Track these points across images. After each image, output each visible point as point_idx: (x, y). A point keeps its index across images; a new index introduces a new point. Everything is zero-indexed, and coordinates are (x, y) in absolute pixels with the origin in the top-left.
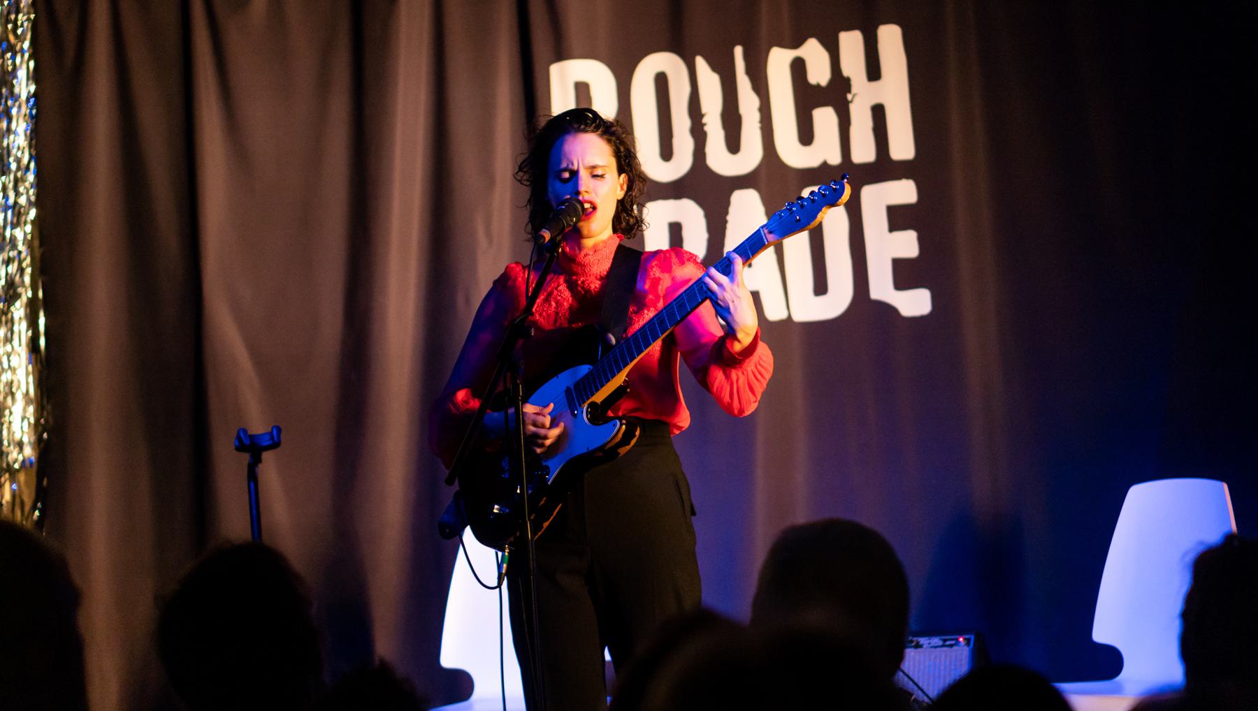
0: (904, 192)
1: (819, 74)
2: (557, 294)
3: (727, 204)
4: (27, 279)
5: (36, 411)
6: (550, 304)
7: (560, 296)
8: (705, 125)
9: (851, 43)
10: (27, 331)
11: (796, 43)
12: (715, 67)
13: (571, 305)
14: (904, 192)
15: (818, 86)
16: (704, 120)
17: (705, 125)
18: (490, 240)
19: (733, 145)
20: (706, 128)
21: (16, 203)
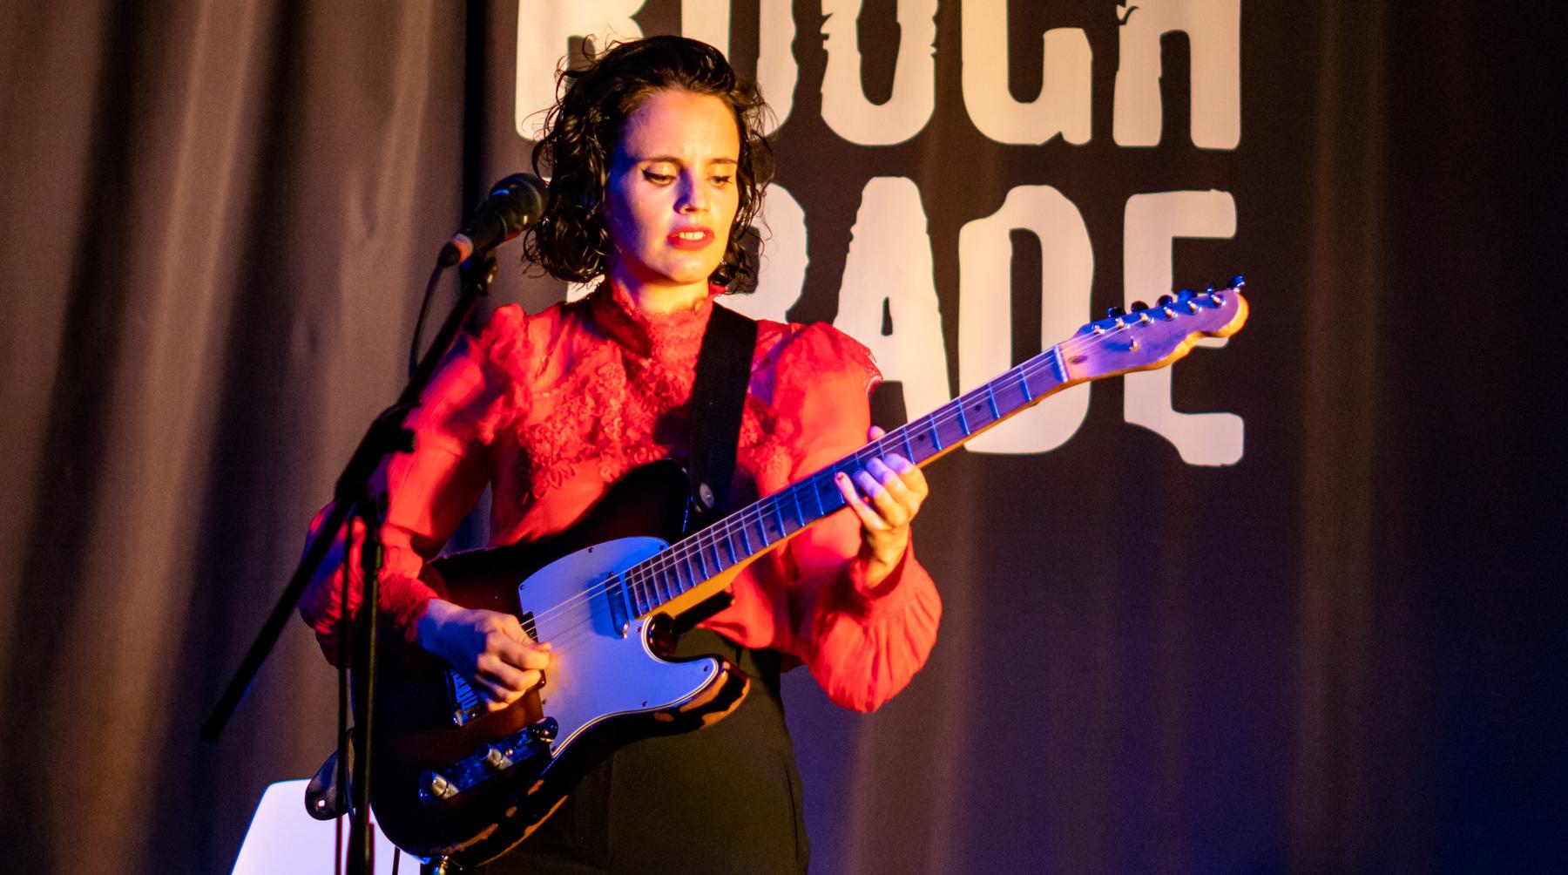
2: (598, 382)
3: (857, 202)
7: (602, 385)
8: (826, 37)
16: (824, 30)
17: (826, 37)
19: (878, 85)
20: (826, 45)
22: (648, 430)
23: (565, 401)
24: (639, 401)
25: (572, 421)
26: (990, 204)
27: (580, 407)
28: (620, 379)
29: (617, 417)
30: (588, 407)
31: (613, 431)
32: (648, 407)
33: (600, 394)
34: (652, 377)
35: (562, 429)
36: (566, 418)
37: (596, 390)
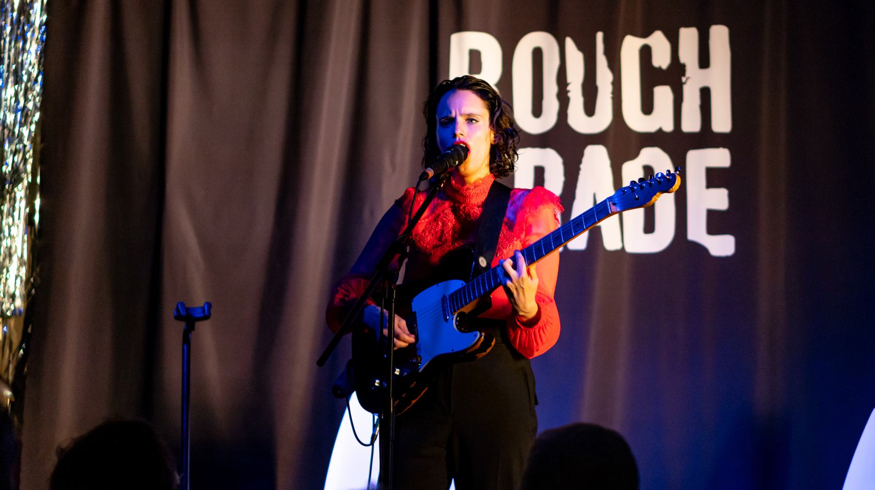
0: (721, 158)
1: (661, 59)
2: (443, 216)
3: (581, 155)
4: (29, 168)
5: (27, 271)
6: (438, 224)
7: (445, 217)
8: (569, 91)
9: (689, 37)
10: (26, 208)
11: (646, 34)
12: (580, 47)
13: (453, 225)
14: (721, 158)
15: (660, 69)
16: (569, 88)
17: (569, 91)
18: (394, 169)
19: (590, 109)
20: (570, 95)
21: (25, 107)
23: (430, 224)
25: (433, 231)
26: (634, 155)
31: (449, 236)
33: (445, 221)
35: (428, 236)
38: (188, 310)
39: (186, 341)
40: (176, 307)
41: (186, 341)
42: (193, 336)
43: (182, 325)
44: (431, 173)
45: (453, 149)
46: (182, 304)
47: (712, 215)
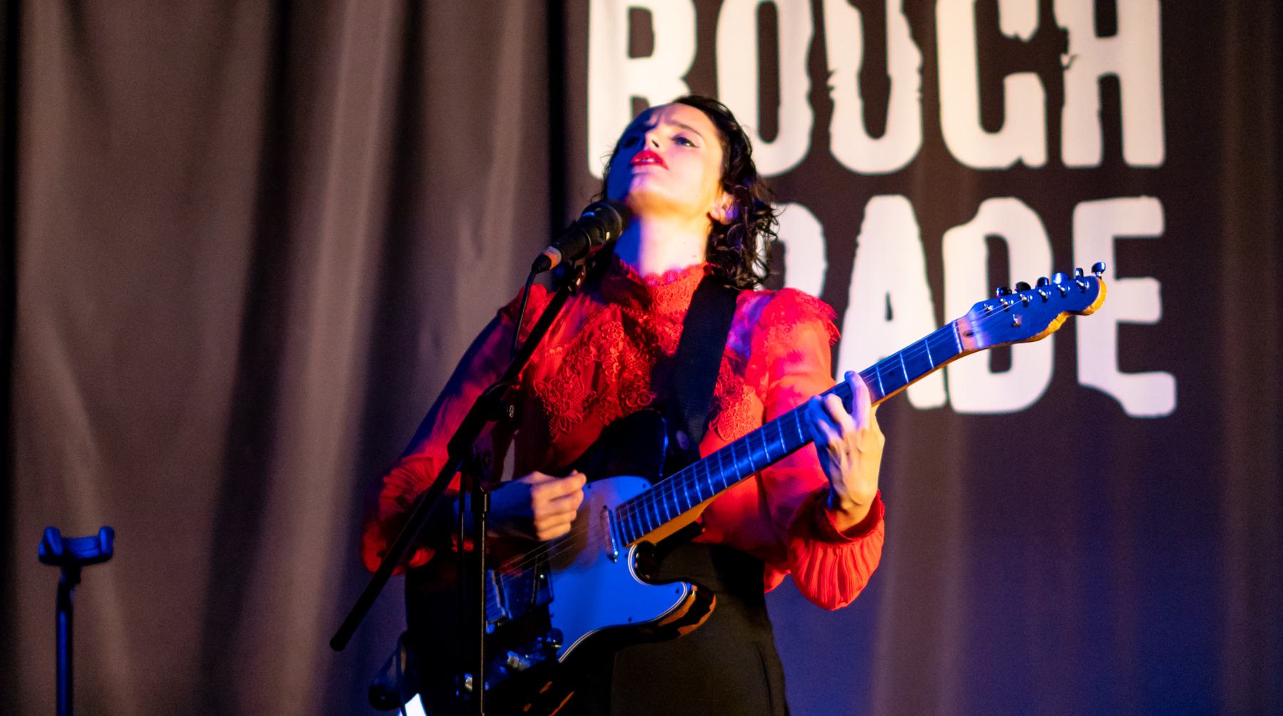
3: (860, 216)
6: (589, 351)
7: (605, 338)
13: (620, 352)
16: (832, 81)
18: (479, 249)
19: (875, 123)
20: (834, 95)
22: (640, 373)
23: (573, 352)
24: (634, 351)
26: (966, 214)
27: (585, 355)
28: (619, 333)
29: (615, 362)
30: (592, 355)
32: (641, 356)
33: (602, 345)
34: (644, 330)
36: (573, 366)
37: (599, 342)
38: (66, 542)
39: (65, 605)
40: (40, 539)
41: (65, 605)
42: (77, 595)
43: (52, 576)
44: (555, 257)
45: (598, 209)
46: (55, 532)
47: (1127, 332)
